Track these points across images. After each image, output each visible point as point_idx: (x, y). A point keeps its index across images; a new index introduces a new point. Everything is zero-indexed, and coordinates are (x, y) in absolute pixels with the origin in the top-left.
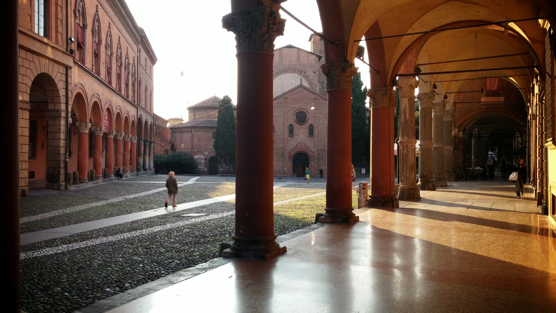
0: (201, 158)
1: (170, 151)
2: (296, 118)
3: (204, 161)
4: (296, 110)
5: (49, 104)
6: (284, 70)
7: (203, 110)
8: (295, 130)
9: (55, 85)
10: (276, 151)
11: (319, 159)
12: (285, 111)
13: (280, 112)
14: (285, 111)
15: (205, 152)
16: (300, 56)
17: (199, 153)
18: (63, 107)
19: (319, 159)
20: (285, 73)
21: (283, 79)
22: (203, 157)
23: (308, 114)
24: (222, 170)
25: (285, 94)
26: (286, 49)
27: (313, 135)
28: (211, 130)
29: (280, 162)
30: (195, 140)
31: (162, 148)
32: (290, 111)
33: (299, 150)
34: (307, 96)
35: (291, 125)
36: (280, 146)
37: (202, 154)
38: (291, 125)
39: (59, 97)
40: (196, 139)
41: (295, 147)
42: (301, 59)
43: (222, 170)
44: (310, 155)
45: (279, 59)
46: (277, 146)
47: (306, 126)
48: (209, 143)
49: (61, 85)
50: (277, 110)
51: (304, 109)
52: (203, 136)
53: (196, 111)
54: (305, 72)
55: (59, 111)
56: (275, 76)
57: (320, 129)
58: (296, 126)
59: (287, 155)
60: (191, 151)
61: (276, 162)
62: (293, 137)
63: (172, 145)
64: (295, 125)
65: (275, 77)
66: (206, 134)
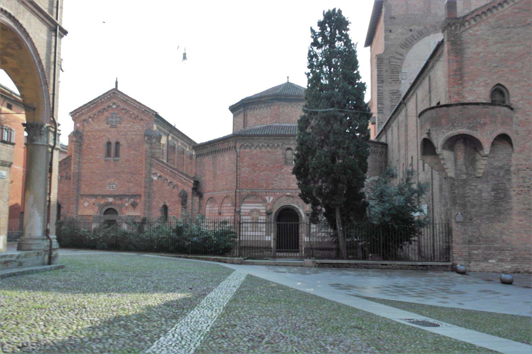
0: (258, 211)
6: (435, 26)
7: (263, 106)
10: (521, 180)
15: (267, 195)
17: (252, 199)
22: (262, 209)
28: (280, 144)
30: (243, 167)
31: (175, 190)
37: (261, 201)
40: (245, 164)
45: (422, 4)
46: (524, 162)
48: (277, 175)
50: (518, 34)
53: (248, 109)
56: (416, 39)
60: (234, 194)
61: (522, 218)
63: (197, 183)
65: (415, 41)
66: (269, 152)
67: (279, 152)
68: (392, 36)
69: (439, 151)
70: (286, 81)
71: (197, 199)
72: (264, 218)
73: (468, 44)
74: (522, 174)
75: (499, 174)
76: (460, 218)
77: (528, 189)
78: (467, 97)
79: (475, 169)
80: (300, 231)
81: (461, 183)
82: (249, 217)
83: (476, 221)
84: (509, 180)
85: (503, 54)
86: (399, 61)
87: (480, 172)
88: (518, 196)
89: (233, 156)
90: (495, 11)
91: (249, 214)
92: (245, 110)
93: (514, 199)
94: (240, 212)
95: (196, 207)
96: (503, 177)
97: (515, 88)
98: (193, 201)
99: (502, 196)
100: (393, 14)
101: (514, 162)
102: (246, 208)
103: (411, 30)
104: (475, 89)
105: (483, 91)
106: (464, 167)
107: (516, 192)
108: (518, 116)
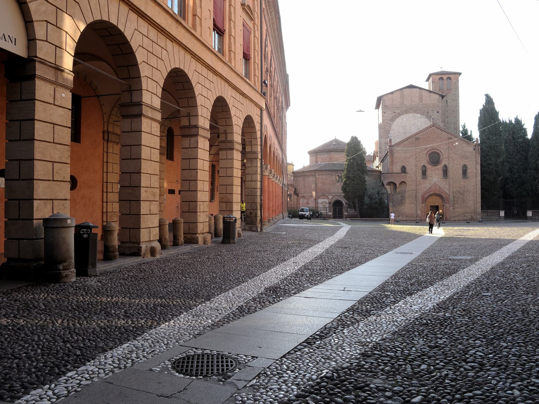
1: (293, 195)
2: (429, 159)
3: (328, 205)
5: (246, 147)
7: (325, 153)
9: (254, 127)
11: (454, 201)
12: (418, 151)
13: (412, 153)
14: (418, 151)
16: (422, 96)
17: (323, 197)
18: (259, 147)
19: (454, 201)
20: (407, 113)
21: (405, 119)
22: (327, 201)
23: (442, 155)
24: (346, 214)
25: (417, 134)
26: (407, 89)
27: (447, 176)
28: (334, 174)
29: (412, 205)
34: (440, 136)
35: (424, 166)
36: (412, 188)
39: (256, 138)
41: (429, 189)
42: (423, 99)
43: (346, 214)
47: (440, 167)
48: (333, 187)
49: (258, 127)
51: (438, 150)
52: (327, 180)
54: (428, 112)
55: (256, 153)
59: (420, 198)
62: (426, 178)
64: (429, 166)
67: (334, 177)
68: (386, 115)
69: (385, 186)
70: (334, 138)
71: (296, 197)
72: (328, 205)
74: (409, 192)
76: (391, 205)
79: (396, 191)
80: (343, 210)
82: (322, 205)
83: (396, 206)
86: (389, 127)
87: (397, 192)
89: (314, 179)
90: (403, 143)
91: (321, 204)
92: (316, 155)
93: (407, 199)
94: (317, 203)
95: (296, 200)
98: (294, 197)
100: (386, 104)
102: (320, 201)
103: (394, 112)
108: (408, 175)
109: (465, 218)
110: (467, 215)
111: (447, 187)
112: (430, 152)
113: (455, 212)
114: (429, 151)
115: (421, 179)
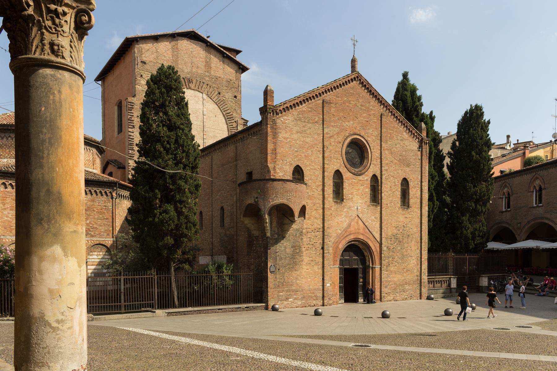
4: (347, 134)
8: (346, 185)
10: (309, 239)
14: (327, 133)
32: (335, 137)
33: (352, 237)
35: (338, 174)
36: (316, 226)
38: (338, 174)
41: (346, 230)
44: (373, 248)
46: (310, 227)
47: (366, 178)
57: (391, 187)
58: (346, 176)
61: (308, 267)
73: (280, 129)
75: (296, 235)
77: (312, 246)
78: (279, 173)
81: (274, 241)
84: (302, 239)
85: (301, 143)
88: (307, 251)
96: (299, 237)
97: (307, 170)
99: (298, 251)
101: (305, 226)
104: (284, 167)
105: (289, 170)
106: (276, 228)
107: (305, 249)
109: (405, 293)
110: (407, 287)
111: (378, 225)
112: (349, 140)
113: (390, 281)
114: (347, 137)
115: (333, 203)
